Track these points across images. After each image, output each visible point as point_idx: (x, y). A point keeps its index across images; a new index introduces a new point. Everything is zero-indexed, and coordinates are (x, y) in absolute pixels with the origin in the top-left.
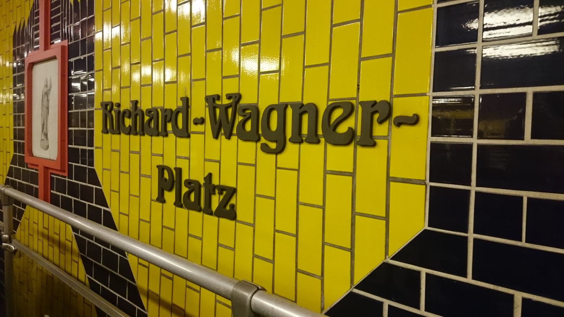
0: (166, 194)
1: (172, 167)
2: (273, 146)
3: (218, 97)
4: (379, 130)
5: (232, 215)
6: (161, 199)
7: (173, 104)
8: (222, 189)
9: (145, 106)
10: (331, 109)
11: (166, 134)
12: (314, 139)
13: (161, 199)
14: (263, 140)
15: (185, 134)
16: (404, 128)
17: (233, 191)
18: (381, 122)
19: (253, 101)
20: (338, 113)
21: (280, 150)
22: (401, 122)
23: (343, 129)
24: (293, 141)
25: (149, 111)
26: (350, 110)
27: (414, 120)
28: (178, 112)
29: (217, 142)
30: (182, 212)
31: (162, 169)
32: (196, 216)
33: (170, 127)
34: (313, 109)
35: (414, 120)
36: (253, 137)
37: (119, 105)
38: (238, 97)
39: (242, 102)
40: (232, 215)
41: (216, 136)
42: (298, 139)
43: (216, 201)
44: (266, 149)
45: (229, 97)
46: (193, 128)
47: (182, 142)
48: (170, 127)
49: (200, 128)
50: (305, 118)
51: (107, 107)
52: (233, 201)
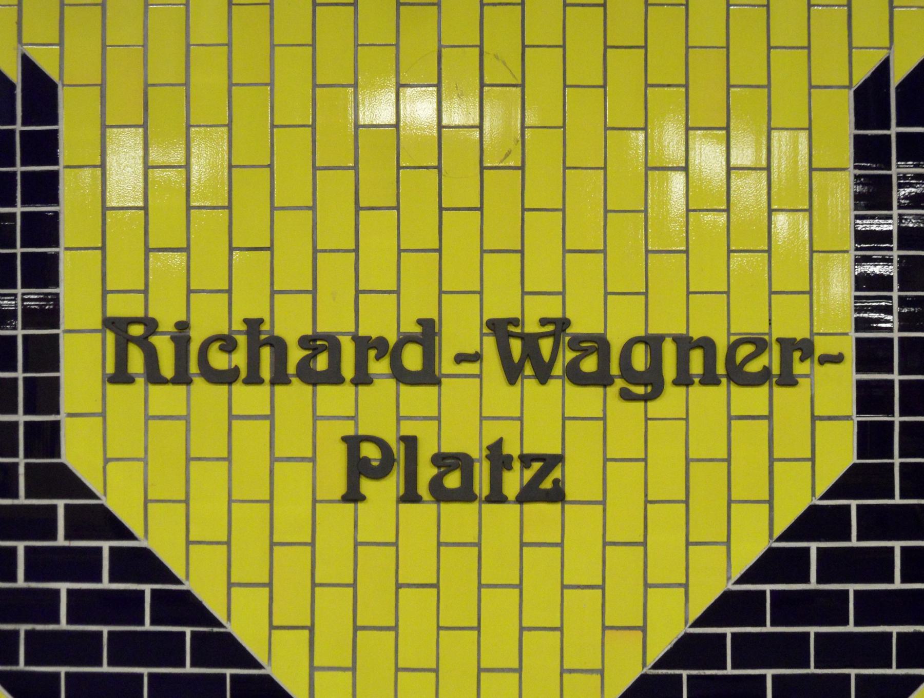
2: (640, 390)
3: (514, 322)
4: (800, 368)
5: (557, 495)
6: (353, 496)
8: (527, 460)
11: (363, 378)
12: (709, 378)
13: (353, 496)
14: (620, 383)
16: (829, 367)
17: (552, 461)
18: (802, 360)
19: (595, 328)
20: (744, 351)
22: (826, 359)
23: (754, 367)
24: (676, 383)
25: (304, 342)
26: (760, 344)
27: (837, 359)
29: (517, 389)
31: (353, 443)
33: (379, 367)
34: (707, 345)
35: (837, 359)
38: (563, 324)
39: (573, 330)
40: (557, 495)
42: (684, 379)
44: (626, 395)
45: (544, 322)
48: (379, 367)
52: (556, 474)
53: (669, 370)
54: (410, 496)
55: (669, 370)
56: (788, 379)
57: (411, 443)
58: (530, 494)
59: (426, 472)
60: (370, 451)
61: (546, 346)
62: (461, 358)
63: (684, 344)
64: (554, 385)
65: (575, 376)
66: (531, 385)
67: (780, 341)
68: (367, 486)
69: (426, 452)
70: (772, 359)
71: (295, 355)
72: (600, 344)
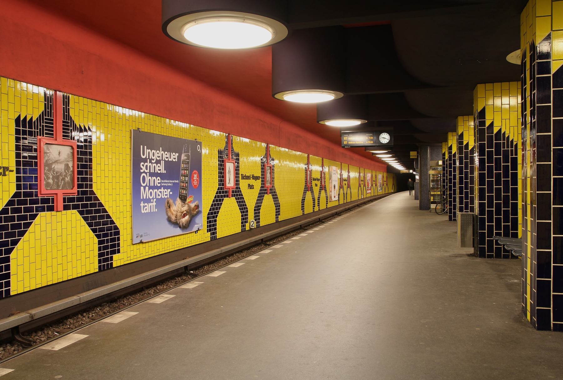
4: (7, 173)
16: (11, 172)
18: (7, 171)
22: (11, 171)
27: (12, 171)
35: (12, 171)
56: (5, 175)
67: (3, 167)
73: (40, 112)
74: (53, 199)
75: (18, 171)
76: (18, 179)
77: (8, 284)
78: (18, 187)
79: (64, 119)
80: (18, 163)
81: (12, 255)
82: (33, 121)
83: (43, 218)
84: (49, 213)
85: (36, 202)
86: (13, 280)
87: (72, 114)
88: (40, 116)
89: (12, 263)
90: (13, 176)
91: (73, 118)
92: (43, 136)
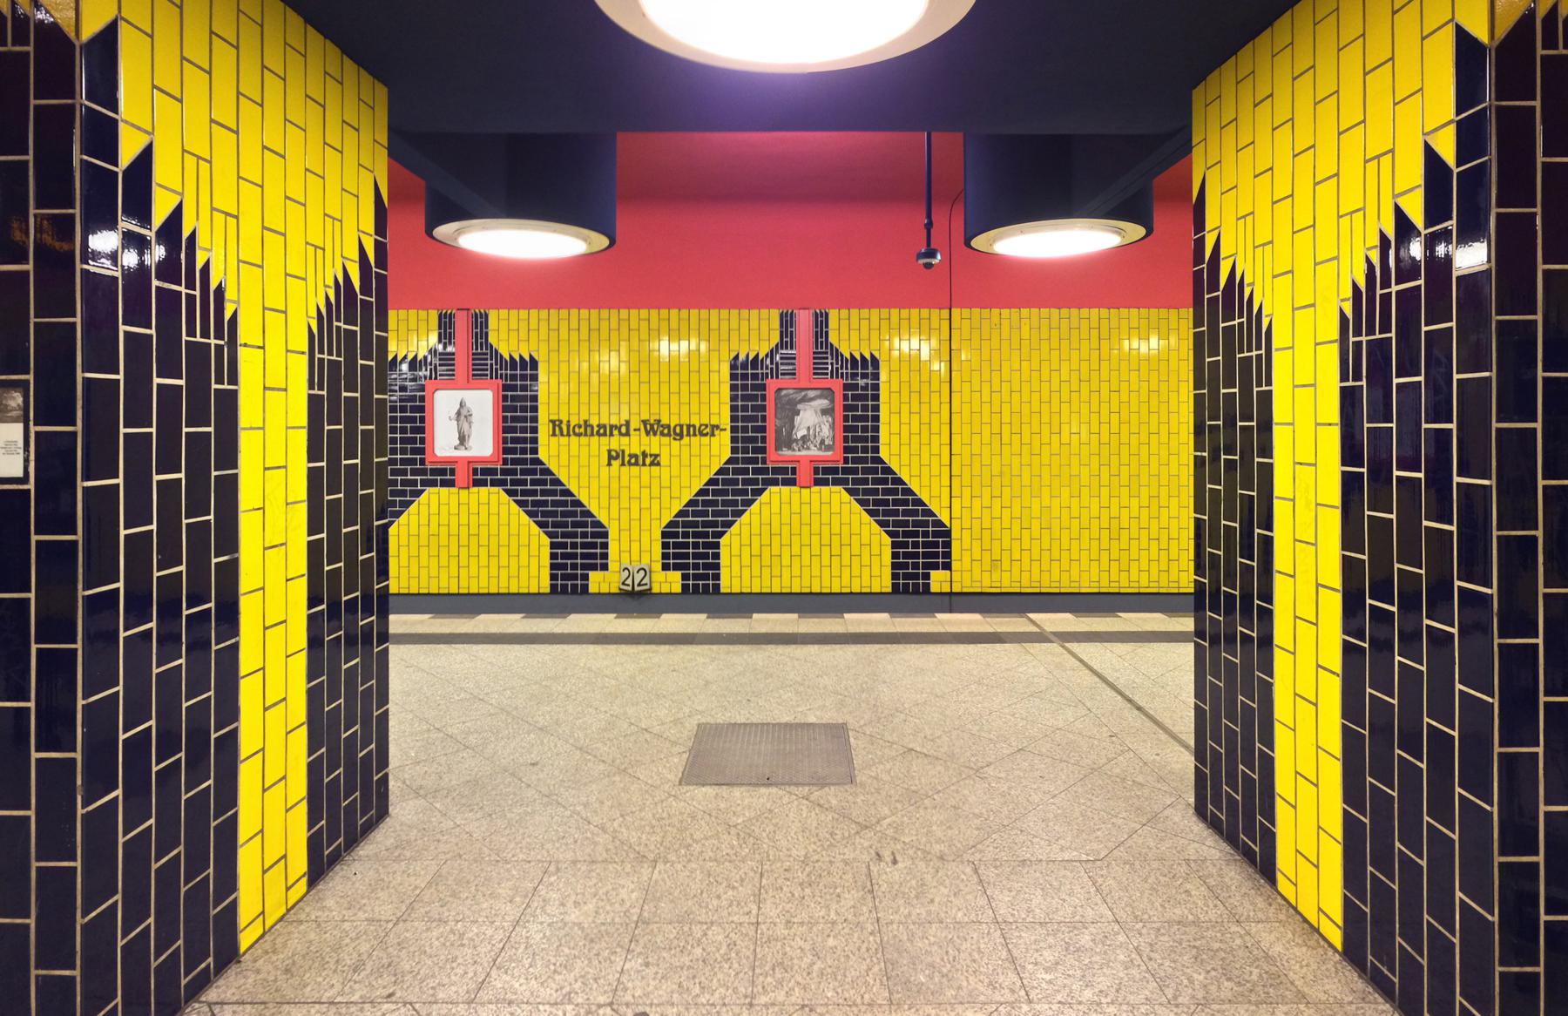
0: (613, 462)
1: (618, 449)
4: (717, 432)
5: (658, 464)
6: (609, 464)
7: (614, 421)
8: (651, 455)
9: (594, 422)
10: (701, 425)
11: (611, 435)
12: (695, 435)
13: (609, 464)
15: (627, 434)
17: (657, 456)
20: (703, 427)
21: (682, 437)
22: (722, 430)
26: (706, 426)
27: (725, 430)
28: (621, 426)
30: (625, 469)
32: (635, 469)
33: (616, 432)
34: (694, 426)
35: (725, 430)
36: (669, 435)
37: (569, 421)
38: (659, 421)
40: (658, 464)
41: (648, 433)
43: (648, 461)
44: (675, 439)
46: (632, 432)
47: (625, 440)
48: (616, 432)
49: (637, 433)
50: (692, 429)
51: (556, 424)
53: (685, 433)
54: (623, 464)
55: (685, 433)
56: (713, 435)
57: (623, 451)
58: (652, 464)
59: (627, 459)
60: (613, 454)
61: (655, 427)
62: (635, 430)
63: (689, 426)
64: (658, 437)
65: (662, 434)
66: (652, 437)
68: (613, 462)
69: (627, 453)
70: (708, 430)
71: (596, 429)
72: (668, 426)
73: (773, 345)
74: (794, 470)
75: (733, 430)
76: (734, 440)
77: (717, 577)
78: (734, 450)
79: (817, 348)
80: (734, 419)
81: (723, 541)
82: (760, 358)
83: (774, 496)
84: (785, 489)
85: (764, 471)
86: (724, 573)
87: (833, 339)
88: (772, 351)
89: (724, 552)
90: (725, 437)
91: (836, 344)
92: (777, 377)
